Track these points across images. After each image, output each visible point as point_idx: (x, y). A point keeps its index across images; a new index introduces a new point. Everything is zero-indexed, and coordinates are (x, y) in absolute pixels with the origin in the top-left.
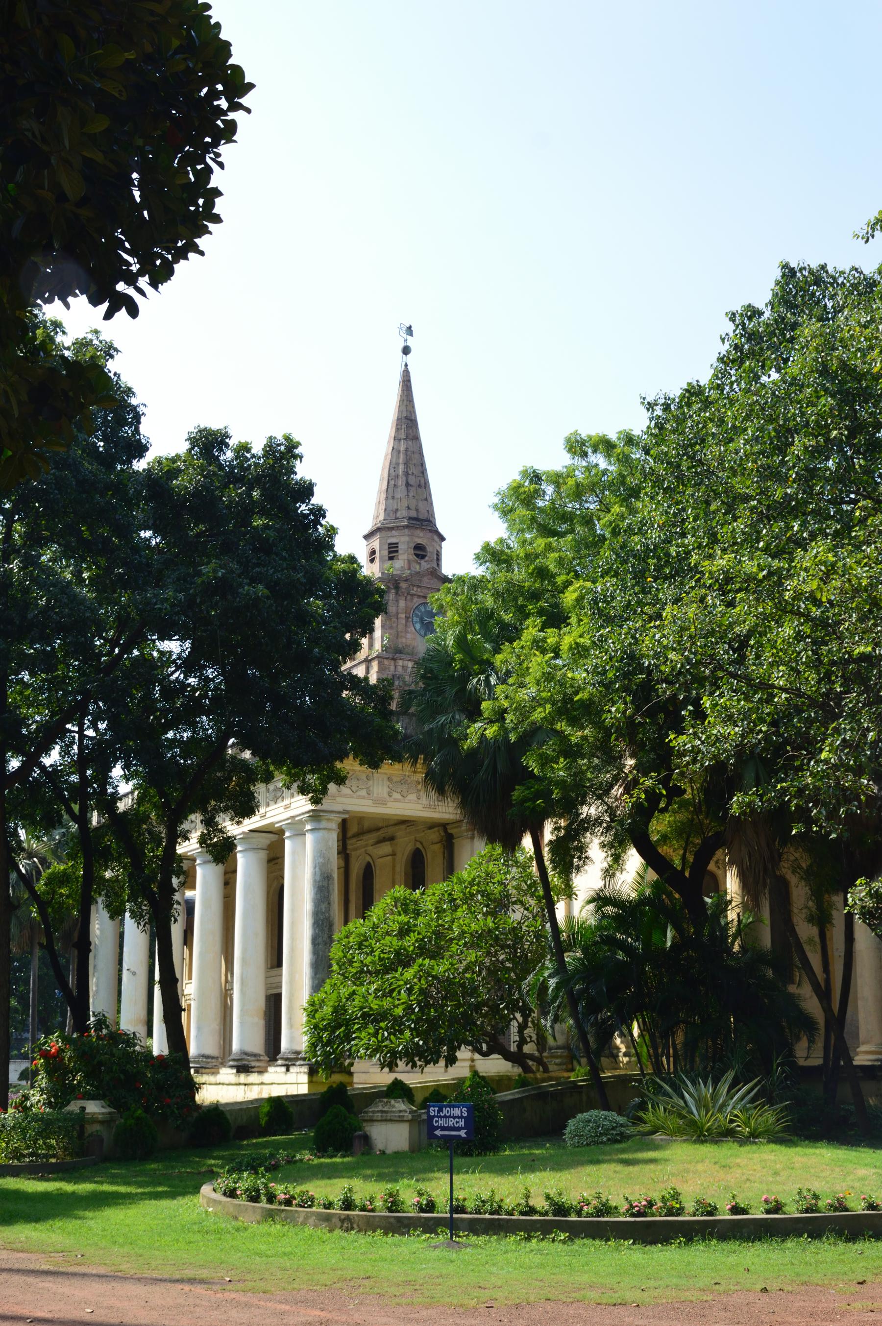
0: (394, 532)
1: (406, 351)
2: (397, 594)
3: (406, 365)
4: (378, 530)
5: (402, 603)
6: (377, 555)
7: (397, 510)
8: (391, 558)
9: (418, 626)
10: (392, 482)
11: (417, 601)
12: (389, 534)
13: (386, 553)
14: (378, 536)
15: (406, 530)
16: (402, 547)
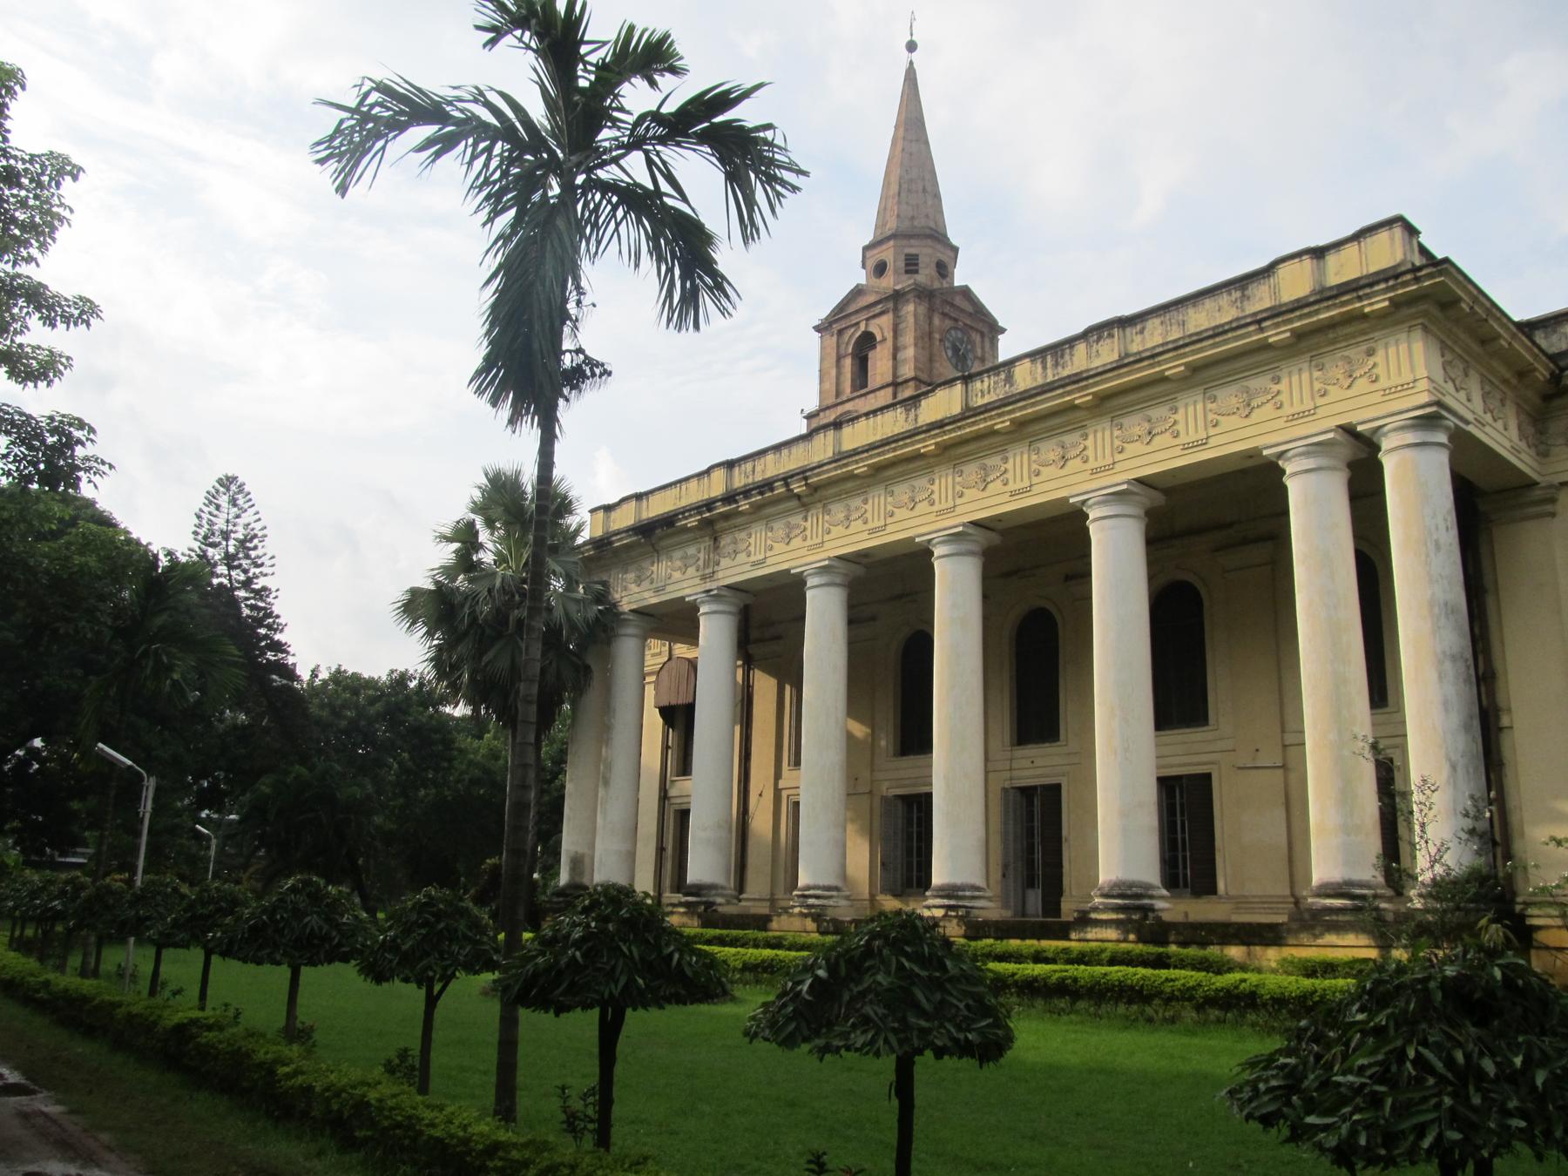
0: (913, 242)
1: (911, 46)
2: (931, 310)
3: (911, 63)
4: (893, 236)
5: (936, 321)
6: (890, 267)
7: (913, 218)
8: (907, 272)
9: (950, 353)
10: (905, 186)
11: (949, 323)
12: (905, 242)
13: (902, 264)
14: (892, 243)
15: (929, 242)
16: (921, 259)
